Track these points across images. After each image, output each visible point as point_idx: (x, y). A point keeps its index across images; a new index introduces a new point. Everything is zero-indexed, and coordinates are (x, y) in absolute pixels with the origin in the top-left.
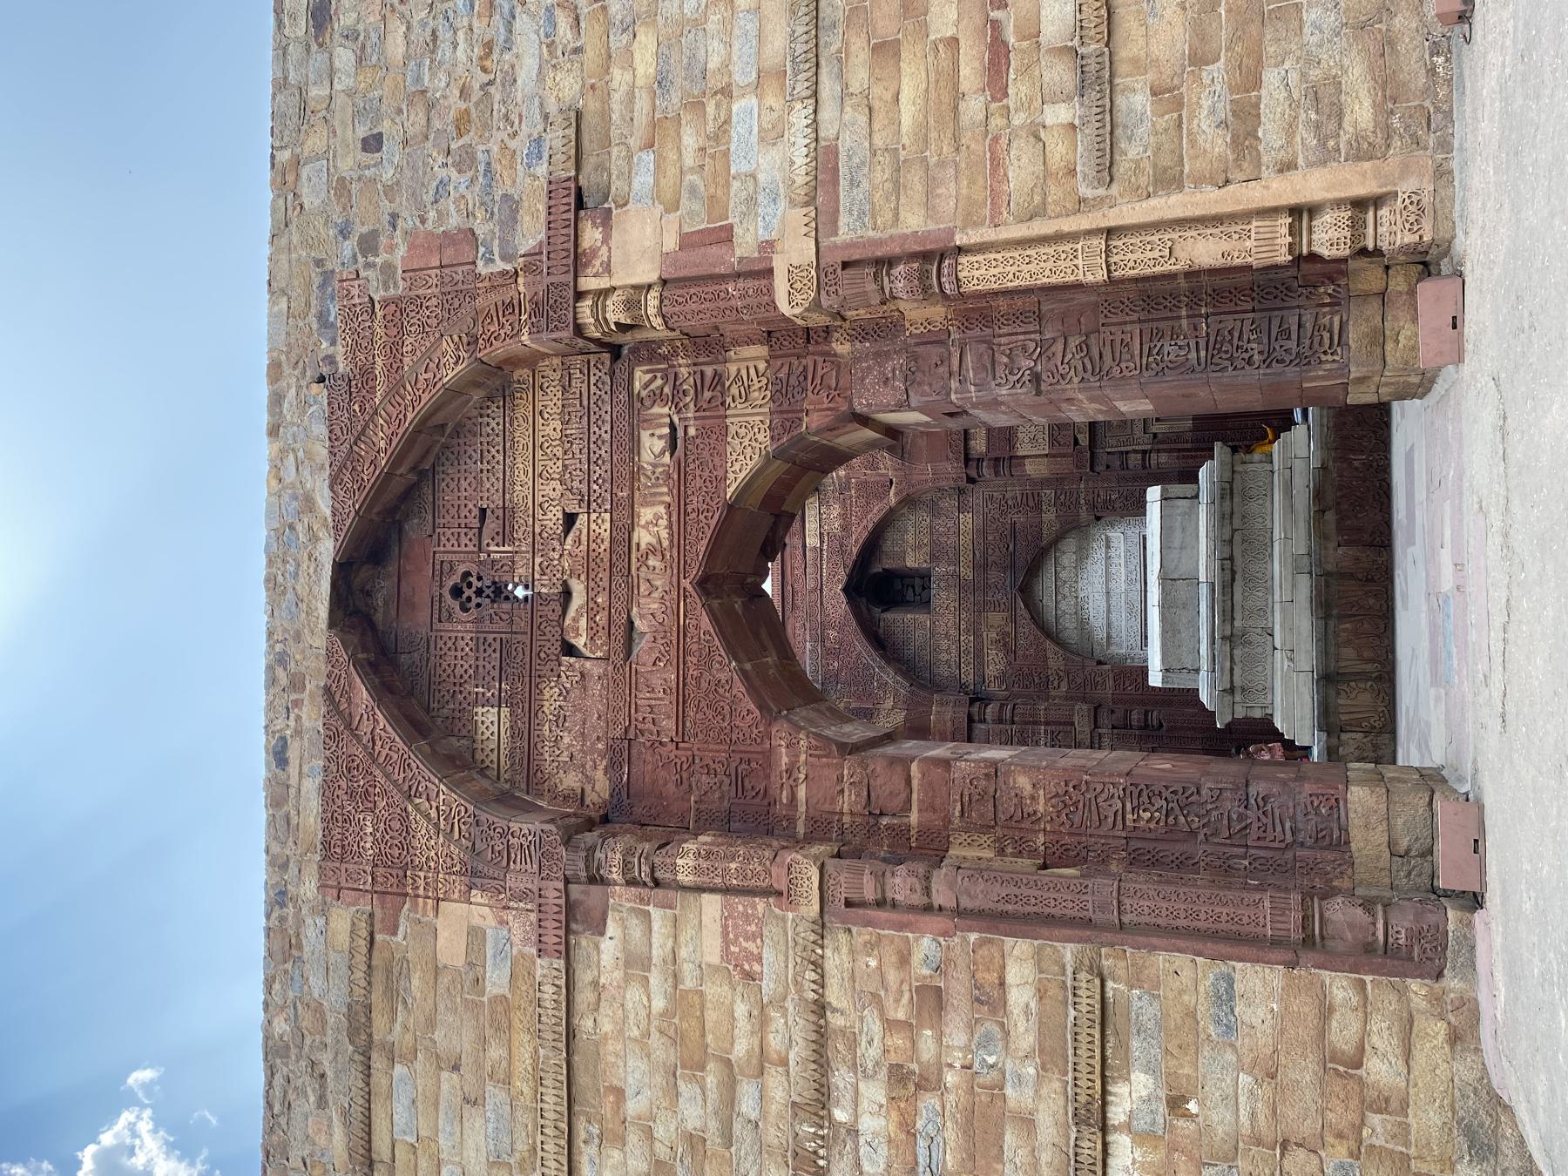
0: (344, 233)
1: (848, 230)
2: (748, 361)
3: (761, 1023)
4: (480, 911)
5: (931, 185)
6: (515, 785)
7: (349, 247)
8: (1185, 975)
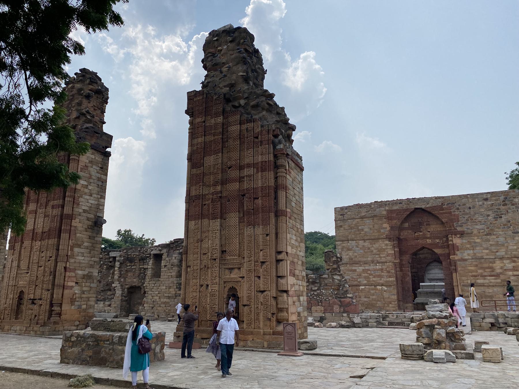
0: (459, 205)
1: (458, 262)
2: (447, 251)
3: (384, 257)
4: (388, 228)
5: (463, 270)
6: (401, 229)
7: (458, 206)
8: (395, 292)
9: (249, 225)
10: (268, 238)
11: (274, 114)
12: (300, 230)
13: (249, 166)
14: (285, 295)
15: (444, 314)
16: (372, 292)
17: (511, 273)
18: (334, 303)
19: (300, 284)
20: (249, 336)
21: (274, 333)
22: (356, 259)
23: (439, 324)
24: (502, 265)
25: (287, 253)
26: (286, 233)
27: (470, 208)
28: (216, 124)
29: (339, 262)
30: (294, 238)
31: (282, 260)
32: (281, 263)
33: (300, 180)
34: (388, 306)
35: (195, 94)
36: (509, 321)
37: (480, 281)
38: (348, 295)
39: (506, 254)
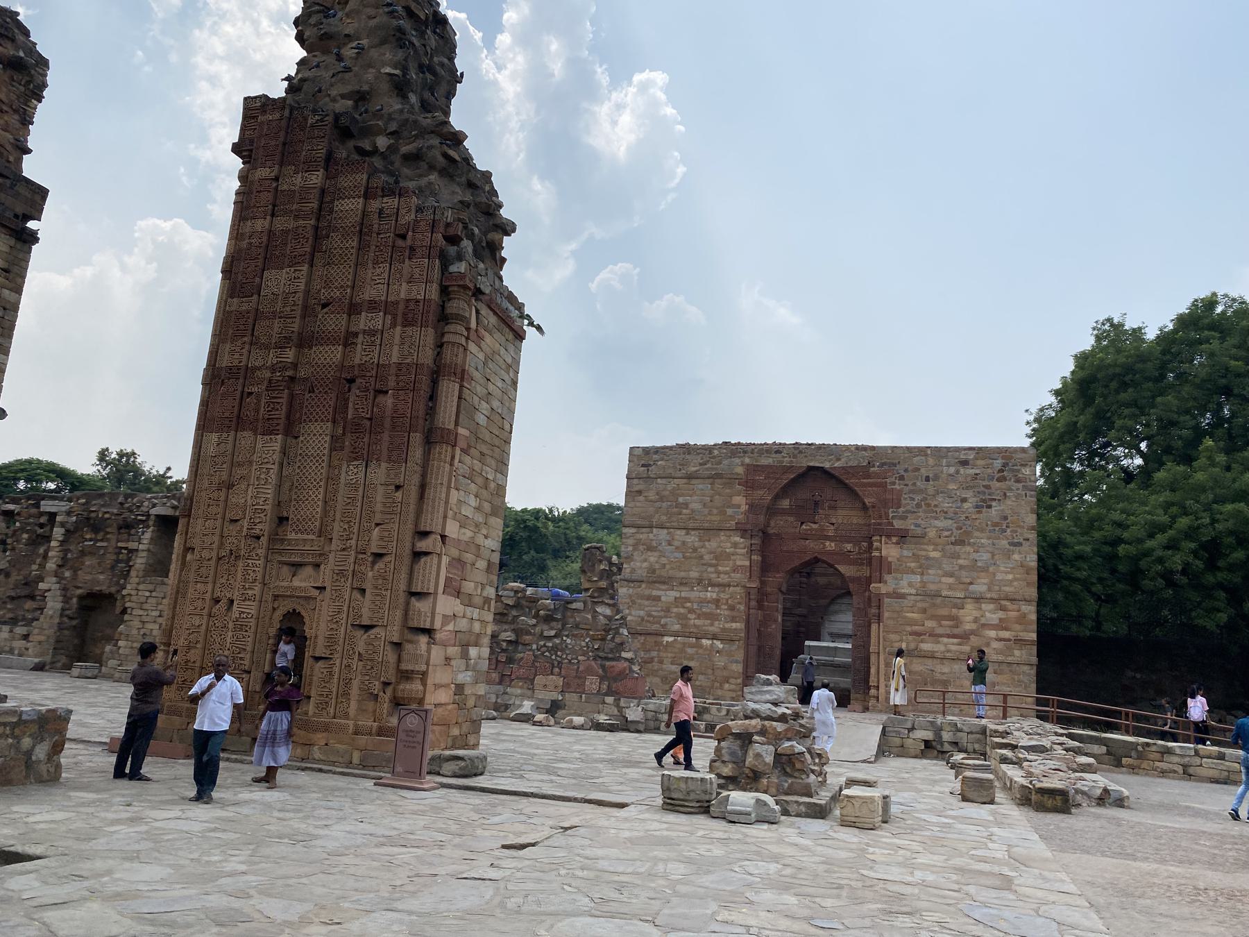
0: (906, 470)
1: (887, 600)
2: (865, 571)
3: (726, 573)
4: (744, 508)
6: (772, 511)
7: (902, 473)
8: (740, 655)
9: (355, 459)
10: (399, 494)
11: (458, 184)
12: (492, 485)
13: (373, 306)
14: (423, 639)
15: (781, 710)
16: (690, 651)
17: (992, 634)
18: (589, 671)
19: (475, 616)
20: (319, 735)
21: (381, 732)
22: (664, 573)
23: (763, 732)
24: (976, 614)
25: (443, 537)
26: (449, 487)
27: (927, 479)
28: (305, 189)
29: (615, 574)
30: (473, 502)
31: (427, 554)
32: (422, 560)
33: (509, 360)
34: (721, 688)
35: (264, 105)
36: (963, 738)
37: (926, 647)
38: (624, 655)
39: (989, 590)
